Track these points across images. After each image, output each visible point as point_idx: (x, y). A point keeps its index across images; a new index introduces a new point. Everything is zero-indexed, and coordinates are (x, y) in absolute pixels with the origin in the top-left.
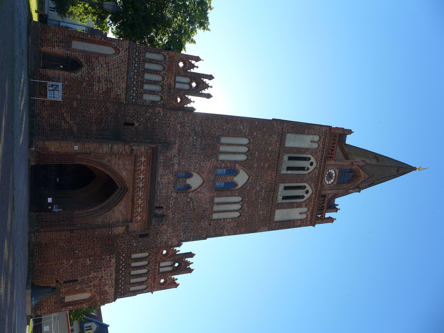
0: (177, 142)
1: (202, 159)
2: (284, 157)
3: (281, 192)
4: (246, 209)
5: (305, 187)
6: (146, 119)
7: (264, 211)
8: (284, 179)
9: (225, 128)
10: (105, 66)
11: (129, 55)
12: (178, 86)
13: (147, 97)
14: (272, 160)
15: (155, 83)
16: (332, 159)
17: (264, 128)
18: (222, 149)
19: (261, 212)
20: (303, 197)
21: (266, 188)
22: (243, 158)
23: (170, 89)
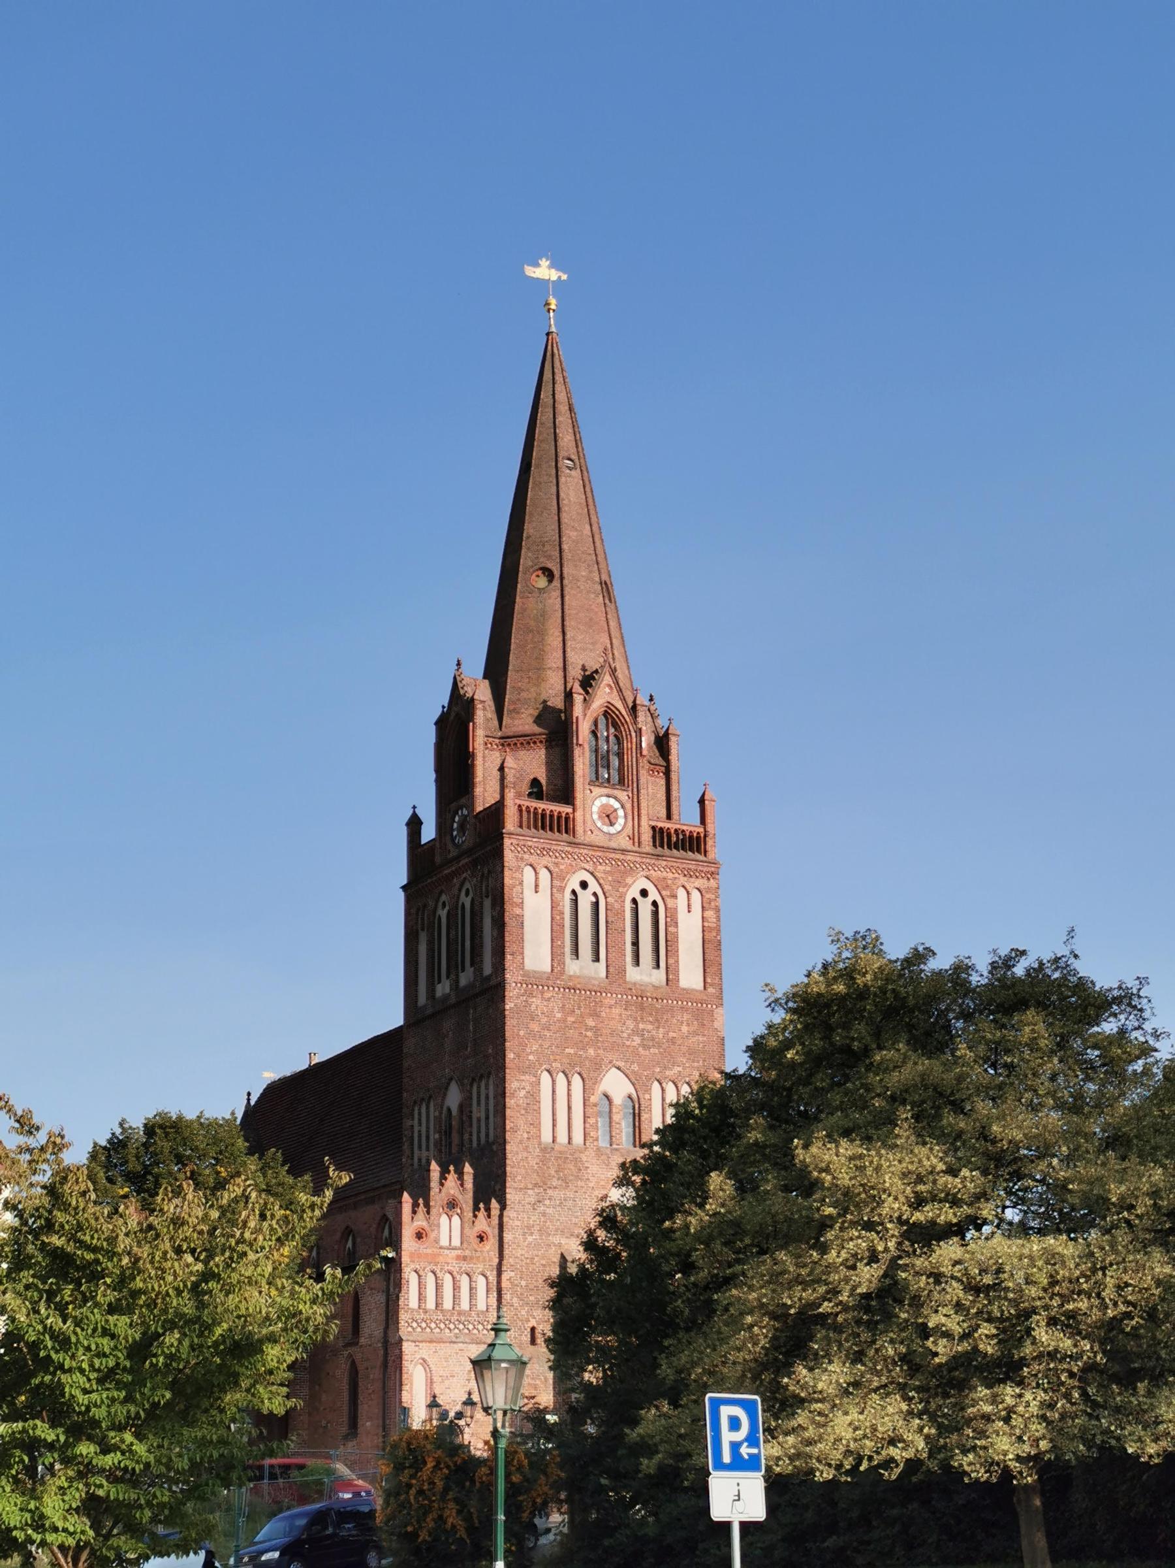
0: (556, 1239)
1: (583, 1184)
2: (572, 973)
3: (645, 975)
4: (677, 1069)
5: (634, 901)
6: (523, 1305)
7: (682, 1022)
8: (615, 973)
9: (526, 1135)
10: (447, 1383)
11: (426, 1342)
12: (456, 1242)
13: (481, 1305)
14: (579, 1008)
15: (456, 1288)
16: (571, 816)
17: (518, 1035)
18: (562, 1138)
19: (685, 1029)
20: (655, 904)
21: (635, 1019)
22: (577, 1081)
23: (465, 1258)
